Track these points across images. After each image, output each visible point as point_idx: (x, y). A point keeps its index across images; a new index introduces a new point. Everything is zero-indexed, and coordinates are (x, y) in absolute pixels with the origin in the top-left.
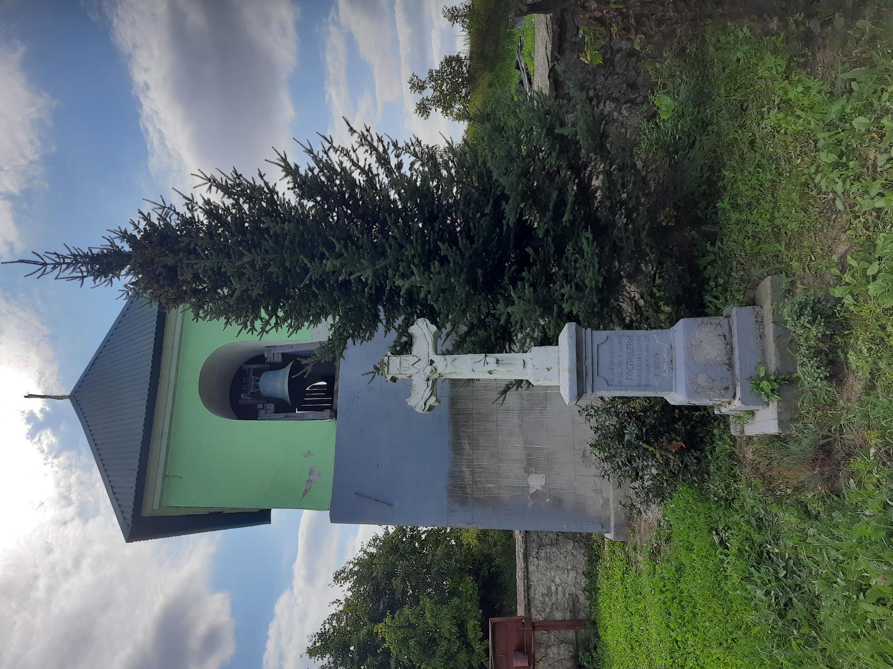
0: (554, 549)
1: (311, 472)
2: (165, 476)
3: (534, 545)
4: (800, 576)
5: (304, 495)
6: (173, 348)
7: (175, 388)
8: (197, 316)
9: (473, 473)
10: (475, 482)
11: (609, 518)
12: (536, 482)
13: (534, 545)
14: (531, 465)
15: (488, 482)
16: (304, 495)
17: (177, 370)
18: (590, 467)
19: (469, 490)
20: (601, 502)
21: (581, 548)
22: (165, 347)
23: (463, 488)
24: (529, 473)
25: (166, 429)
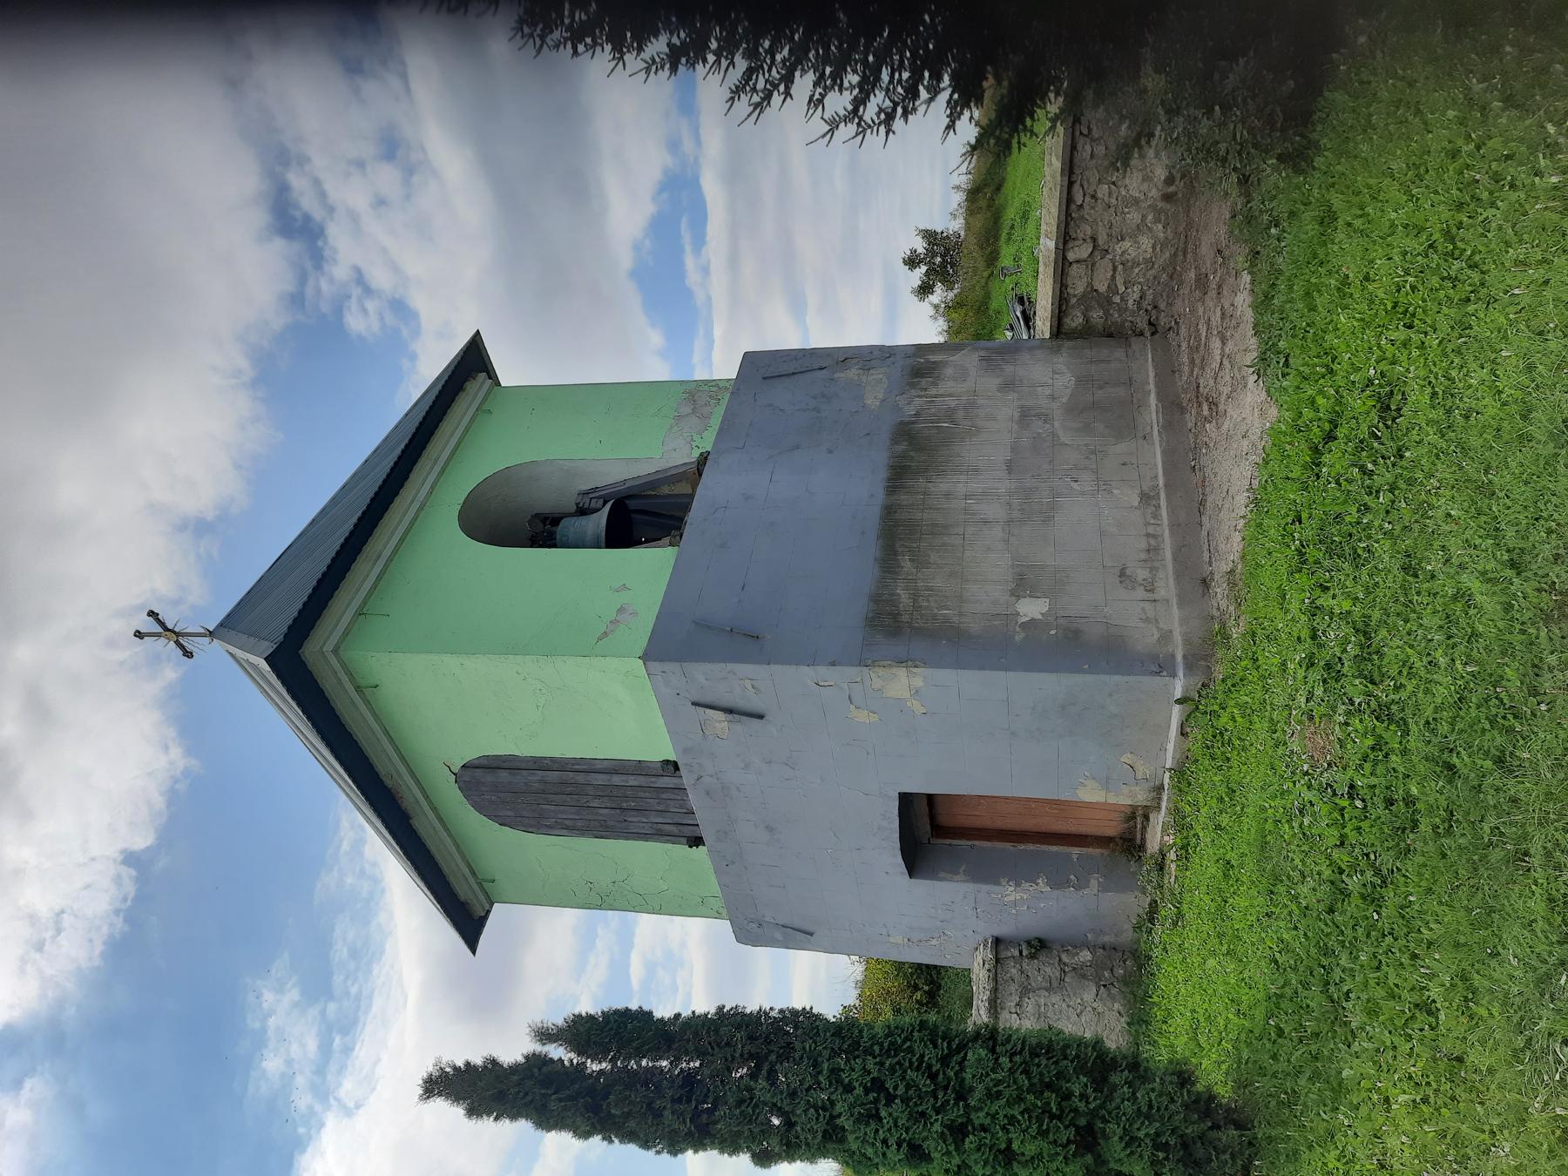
0: (1055, 998)
1: (621, 610)
2: (360, 613)
3: (1013, 988)
4: (1522, 264)
5: (600, 639)
6: (436, 461)
7: (421, 508)
8: (575, 53)
9: (915, 597)
10: (917, 608)
11: (1173, 656)
12: (1032, 608)
13: (1013, 988)
14: (1023, 585)
15: (941, 608)
16: (600, 639)
17: (433, 488)
18: (1133, 588)
19: (905, 618)
20: (1156, 636)
21: (1113, 998)
22: (425, 454)
23: (896, 616)
24: (1019, 597)
25: (387, 553)
